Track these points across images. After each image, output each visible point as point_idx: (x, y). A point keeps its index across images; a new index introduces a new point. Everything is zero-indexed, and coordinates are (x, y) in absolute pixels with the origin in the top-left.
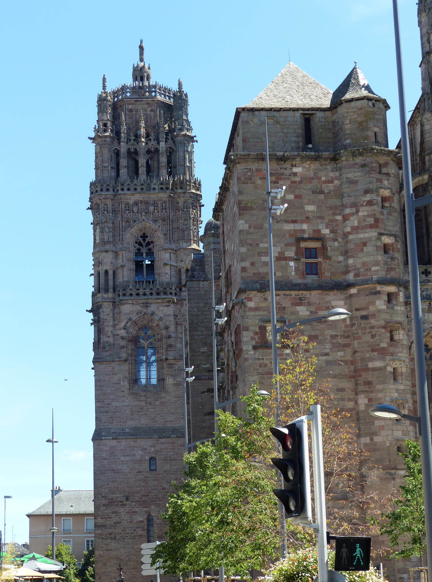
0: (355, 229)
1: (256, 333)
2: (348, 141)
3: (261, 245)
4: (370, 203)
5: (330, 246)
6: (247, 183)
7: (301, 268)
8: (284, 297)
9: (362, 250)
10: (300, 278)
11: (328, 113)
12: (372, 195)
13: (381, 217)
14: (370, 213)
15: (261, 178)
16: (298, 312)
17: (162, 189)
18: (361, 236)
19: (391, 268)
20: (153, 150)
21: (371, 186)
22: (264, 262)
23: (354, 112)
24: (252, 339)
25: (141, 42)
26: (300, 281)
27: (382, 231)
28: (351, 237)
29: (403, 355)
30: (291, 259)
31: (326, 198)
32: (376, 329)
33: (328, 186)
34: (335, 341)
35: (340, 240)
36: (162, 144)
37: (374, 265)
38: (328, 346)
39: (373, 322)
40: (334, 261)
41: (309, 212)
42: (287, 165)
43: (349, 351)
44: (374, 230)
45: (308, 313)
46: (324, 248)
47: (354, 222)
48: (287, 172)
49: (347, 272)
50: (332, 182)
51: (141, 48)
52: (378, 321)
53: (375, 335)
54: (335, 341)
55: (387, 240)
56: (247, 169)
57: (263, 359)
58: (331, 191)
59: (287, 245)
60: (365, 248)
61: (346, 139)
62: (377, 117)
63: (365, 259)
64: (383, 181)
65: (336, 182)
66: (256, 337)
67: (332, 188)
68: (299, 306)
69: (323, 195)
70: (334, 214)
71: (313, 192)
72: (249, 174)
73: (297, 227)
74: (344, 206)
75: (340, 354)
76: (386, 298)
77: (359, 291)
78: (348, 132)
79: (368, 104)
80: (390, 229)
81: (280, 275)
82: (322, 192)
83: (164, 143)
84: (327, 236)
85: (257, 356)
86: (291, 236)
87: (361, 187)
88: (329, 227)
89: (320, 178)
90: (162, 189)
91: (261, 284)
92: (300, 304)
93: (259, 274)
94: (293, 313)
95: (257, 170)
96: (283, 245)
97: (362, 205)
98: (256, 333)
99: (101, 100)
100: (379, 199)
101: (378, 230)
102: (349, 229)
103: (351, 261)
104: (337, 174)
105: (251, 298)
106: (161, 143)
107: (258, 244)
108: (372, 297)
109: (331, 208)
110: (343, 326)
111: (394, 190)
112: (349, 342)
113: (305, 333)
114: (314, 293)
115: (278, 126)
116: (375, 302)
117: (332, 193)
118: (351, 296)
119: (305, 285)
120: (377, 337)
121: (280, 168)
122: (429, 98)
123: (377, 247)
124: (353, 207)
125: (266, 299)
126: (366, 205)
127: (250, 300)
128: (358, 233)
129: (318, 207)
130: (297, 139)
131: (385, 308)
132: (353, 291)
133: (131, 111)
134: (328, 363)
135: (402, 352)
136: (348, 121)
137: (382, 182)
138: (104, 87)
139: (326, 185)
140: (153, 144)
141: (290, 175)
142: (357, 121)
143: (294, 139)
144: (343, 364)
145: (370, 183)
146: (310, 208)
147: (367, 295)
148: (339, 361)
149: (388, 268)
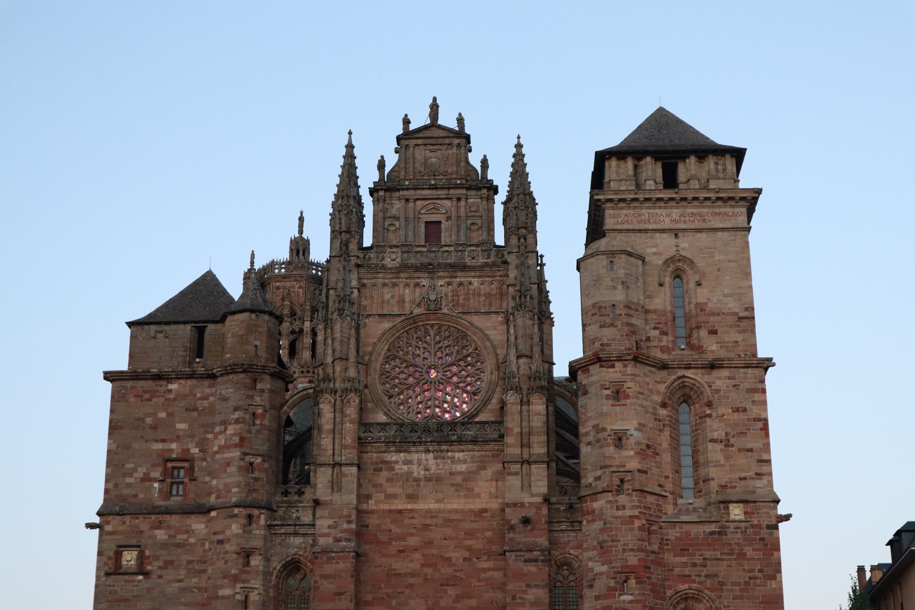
0: (222, 449)
1: (110, 558)
2: (228, 356)
3: (127, 466)
4: (237, 421)
5: (198, 466)
6: (120, 401)
7: (165, 489)
8: (143, 520)
9: (225, 470)
10: (163, 500)
11: (219, 326)
12: (240, 413)
13: (248, 435)
14: (236, 431)
15: (134, 396)
16: (156, 536)
17: (302, 372)
18: (226, 455)
19: (254, 489)
20: (297, 330)
21: (240, 403)
22: (128, 483)
23: (236, 325)
24: (106, 564)
25: (302, 213)
26: (162, 503)
27: (247, 451)
28: (217, 456)
29: (256, 583)
30: (156, 480)
31: (199, 415)
32: (229, 555)
33: (202, 403)
34: (190, 567)
35: (209, 459)
36: (307, 325)
37: (235, 487)
38: (183, 572)
39: (227, 547)
40: (200, 482)
41: (181, 430)
42: (164, 383)
43: (204, 577)
44: (238, 449)
45: (166, 537)
46: (191, 469)
47: (222, 441)
48: (162, 389)
49: (209, 495)
50: (206, 398)
51: (301, 219)
52: (231, 546)
53: (228, 560)
54: (190, 567)
55: (248, 459)
56: (122, 386)
57: (114, 586)
58: (205, 408)
59: (154, 465)
60: (228, 468)
61: (227, 353)
62: (260, 329)
63: (227, 480)
64: (255, 397)
65: (211, 398)
66: (110, 562)
67: (206, 405)
68: (158, 529)
69: (196, 412)
70: (206, 432)
71: (187, 409)
72: (123, 391)
73: (166, 446)
74: (215, 424)
75: (195, 580)
76: (243, 521)
77: (218, 514)
78: (229, 346)
79: (250, 316)
80: (256, 447)
81: (143, 497)
82: (195, 409)
83: (309, 322)
84: (196, 456)
85: (108, 583)
86: (158, 455)
87: (232, 403)
88: (199, 446)
89: (195, 395)
90: (302, 372)
91: (121, 507)
92: (159, 528)
93: (122, 495)
94: (150, 537)
95: (132, 388)
96: (149, 465)
97: (230, 424)
98: (110, 558)
99: (247, 276)
100: (247, 417)
101: (243, 450)
102: (216, 449)
103: (214, 482)
104: (213, 390)
105: (109, 521)
106: (306, 323)
107: (123, 465)
108: (229, 520)
109: (203, 426)
110: (201, 551)
111: (268, 406)
112: (205, 568)
113: (161, 558)
114: (174, 516)
115: (167, 340)
116: (231, 526)
117: (206, 410)
118: (212, 517)
119: (167, 507)
120: (230, 564)
121: (156, 385)
122: (323, 308)
123: (240, 468)
124: (223, 425)
125: (124, 523)
126: (234, 424)
127: (108, 523)
128: (224, 453)
129: (190, 425)
130: (185, 353)
131: (241, 532)
132: (213, 514)
133: (278, 288)
134: (182, 590)
135: (255, 579)
136: (230, 335)
137: (254, 399)
138: (252, 263)
139: (201, 402)
140: (296, 326)
141: (165, 392)
142: (238, 335)
143: (182, 353)
144: (196, 591)
145: (239, 400)
146: (181, 426)
147: (225, 519)
148: (193, 587)
149: (249, 490)
